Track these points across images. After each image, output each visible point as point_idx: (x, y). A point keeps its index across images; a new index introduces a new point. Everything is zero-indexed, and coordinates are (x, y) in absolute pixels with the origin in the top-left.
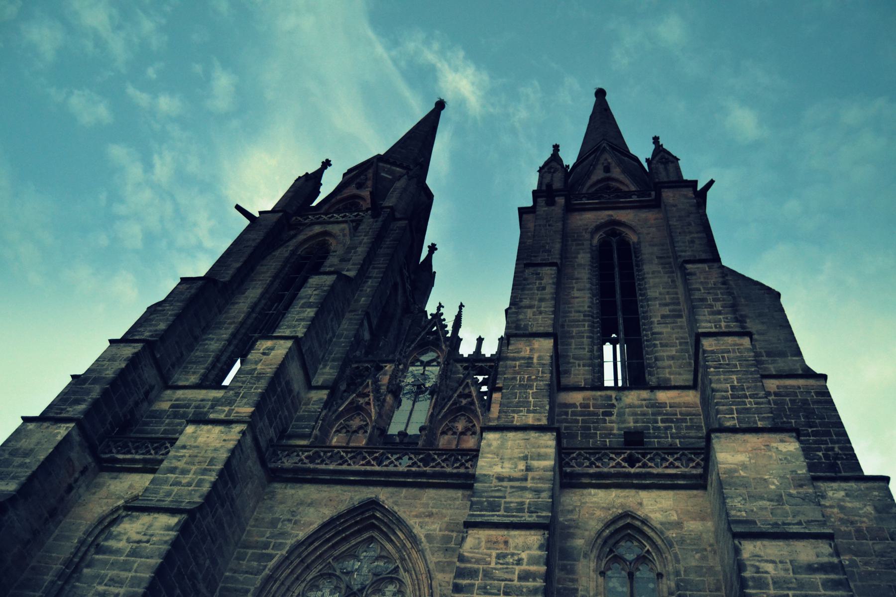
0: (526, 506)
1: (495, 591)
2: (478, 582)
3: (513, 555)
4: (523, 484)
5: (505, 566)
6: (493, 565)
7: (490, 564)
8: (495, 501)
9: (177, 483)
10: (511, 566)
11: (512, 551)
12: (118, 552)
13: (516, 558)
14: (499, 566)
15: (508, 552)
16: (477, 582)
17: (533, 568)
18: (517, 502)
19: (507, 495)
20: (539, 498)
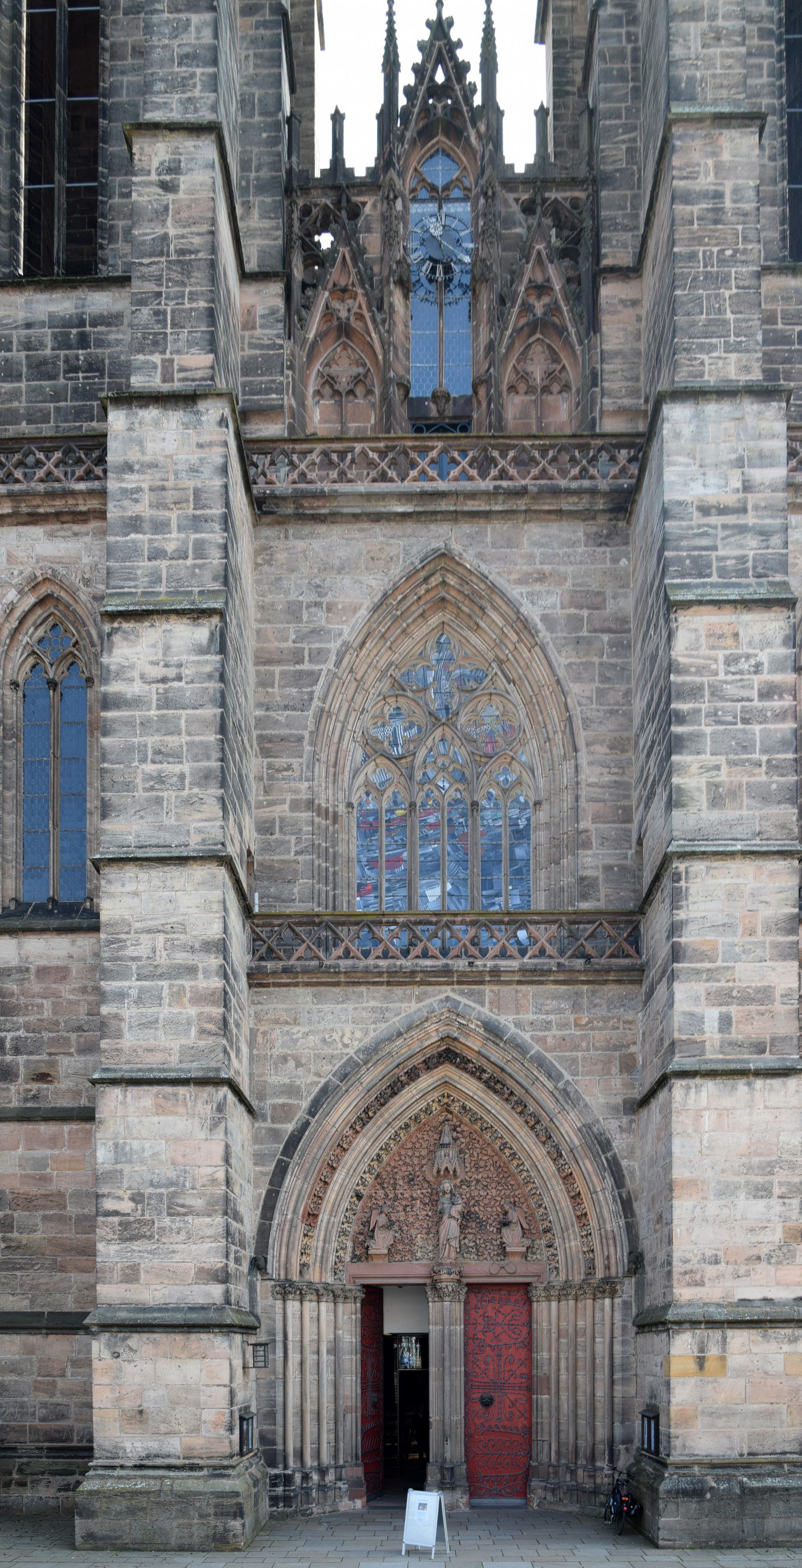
0: (750, 564)
1: (729, 718)
2: (704, 706)
3: (748, 657)
4: (741, 520)
5: (738, 677)
6: (721, 676)
7: (717, 674)
8: (701, 556)
9: (156, 554)
10: (746, 677)
11: (745, 649)
12: (136, 702)
13: (753, 662)
14: (730, 677)
15: (740, 651)
16: (703, 706)
17: (778, 678)
18: (736, 558)
19: (719, 543)
20: (767, 548)
